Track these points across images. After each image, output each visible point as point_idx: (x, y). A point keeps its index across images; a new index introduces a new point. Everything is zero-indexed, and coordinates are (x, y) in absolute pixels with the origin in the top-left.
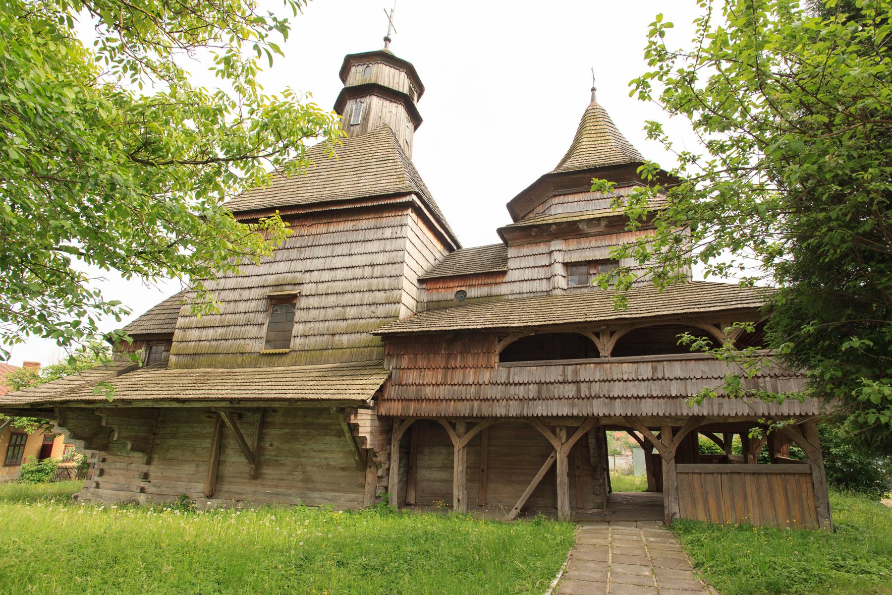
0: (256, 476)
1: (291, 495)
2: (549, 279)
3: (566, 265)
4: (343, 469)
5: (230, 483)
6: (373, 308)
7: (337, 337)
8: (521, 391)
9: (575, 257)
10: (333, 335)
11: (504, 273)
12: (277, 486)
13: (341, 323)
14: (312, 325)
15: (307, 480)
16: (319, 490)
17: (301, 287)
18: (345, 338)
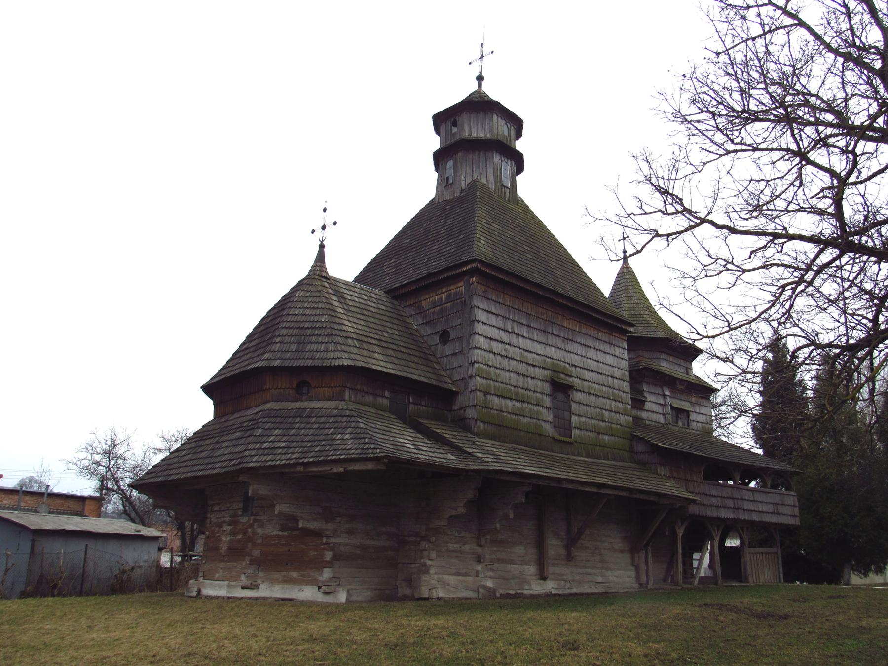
0: (569, 558)
1: (595, 574)
2: (664, 415)
3: (672, 408)
4: (622, 551)
5: (554, 565)
6: (618, 415)
7: (601, 436)
8: (714, 501)
9: (677, 404)
10: (599, 433)
11: (643, 402)
12: (585, 567)
13: (601, 423)
14: (583, 419)
15: (602, 561)
16: (611, 569)
17: (571, 380)
18: (606, 437)
